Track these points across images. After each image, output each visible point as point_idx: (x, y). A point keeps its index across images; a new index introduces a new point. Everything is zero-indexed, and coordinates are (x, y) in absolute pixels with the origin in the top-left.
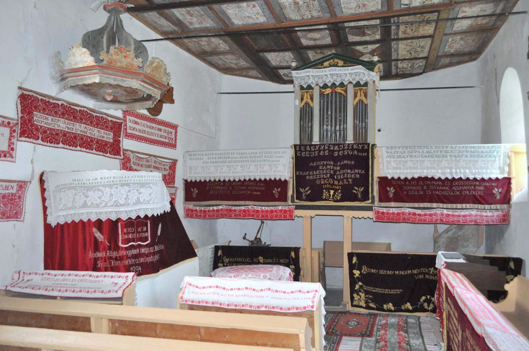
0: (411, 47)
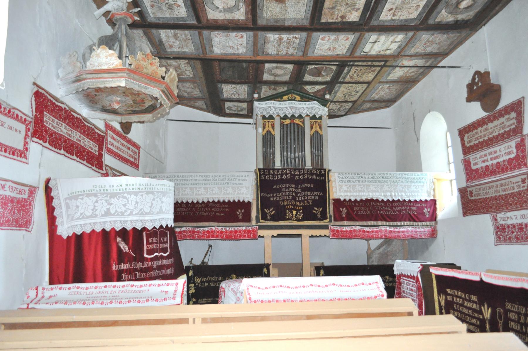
0: (349, 91)
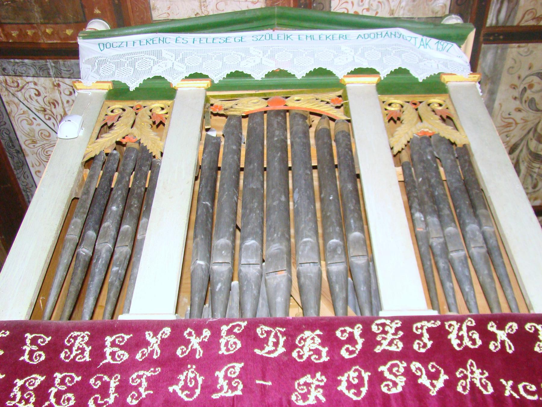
0: (531, 116)
